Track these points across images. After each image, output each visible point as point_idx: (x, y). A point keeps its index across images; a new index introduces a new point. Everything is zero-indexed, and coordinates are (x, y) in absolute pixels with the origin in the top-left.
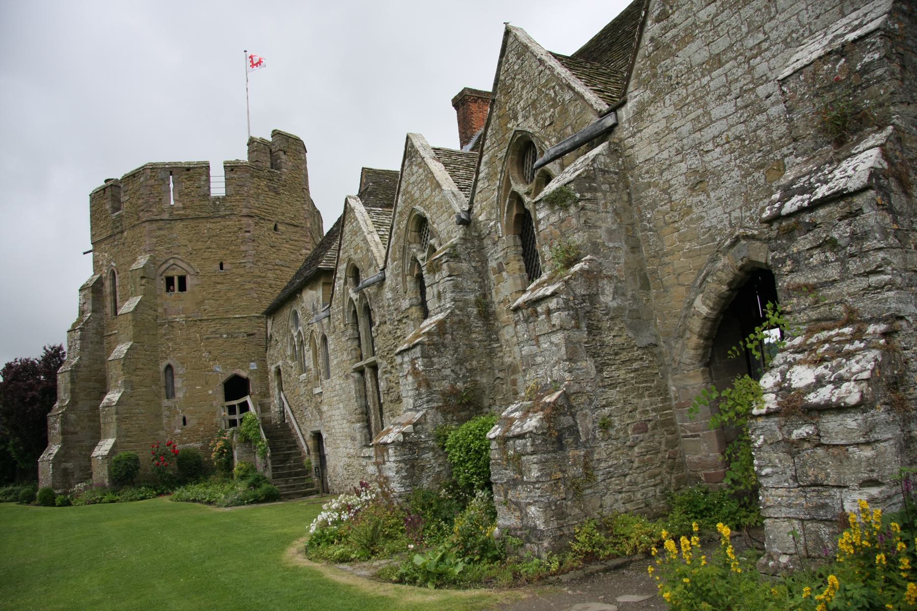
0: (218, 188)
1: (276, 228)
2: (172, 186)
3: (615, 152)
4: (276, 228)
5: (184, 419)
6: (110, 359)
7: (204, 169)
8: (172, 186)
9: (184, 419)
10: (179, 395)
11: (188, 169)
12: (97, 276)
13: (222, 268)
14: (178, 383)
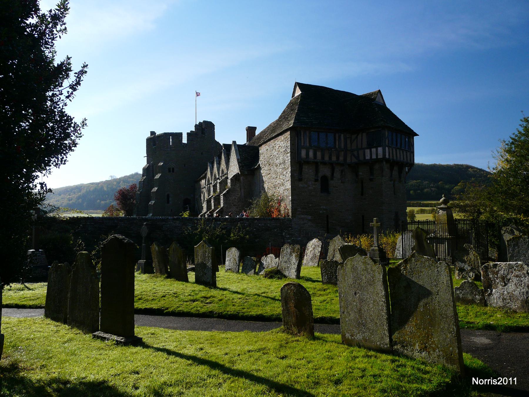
0: (185, 140)
1: (202, 154)
2: (171, 140)
3: (227, 178)
4: (202, 154)
5: (172, 210)
6: (152, 191)
7: (180, 134)
8: (171, 140)
9: (172, 210)
10: (170, 203)
11: (176, 135)
12: (148, 165)
13: (185, 166)
14: (170, 199)
